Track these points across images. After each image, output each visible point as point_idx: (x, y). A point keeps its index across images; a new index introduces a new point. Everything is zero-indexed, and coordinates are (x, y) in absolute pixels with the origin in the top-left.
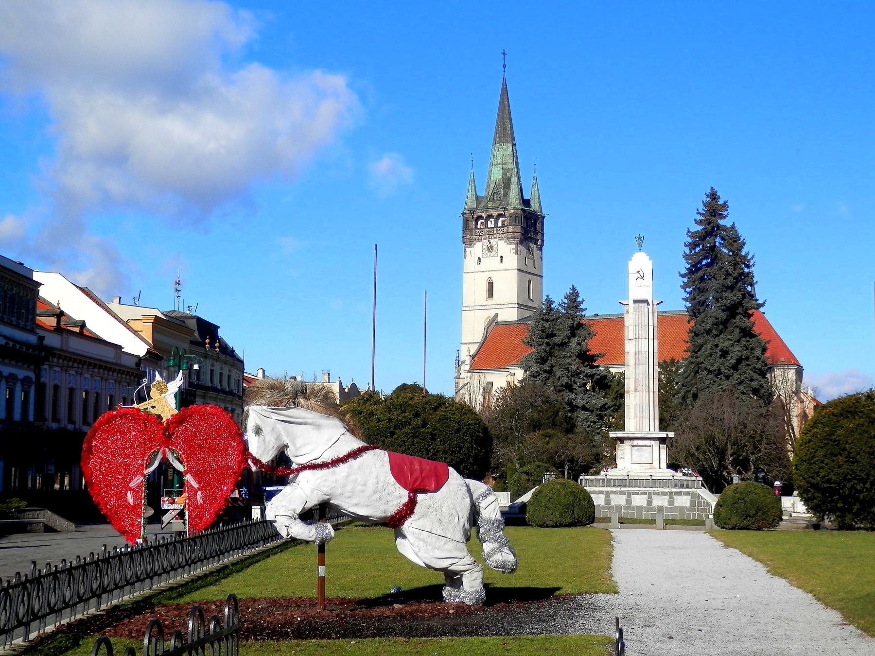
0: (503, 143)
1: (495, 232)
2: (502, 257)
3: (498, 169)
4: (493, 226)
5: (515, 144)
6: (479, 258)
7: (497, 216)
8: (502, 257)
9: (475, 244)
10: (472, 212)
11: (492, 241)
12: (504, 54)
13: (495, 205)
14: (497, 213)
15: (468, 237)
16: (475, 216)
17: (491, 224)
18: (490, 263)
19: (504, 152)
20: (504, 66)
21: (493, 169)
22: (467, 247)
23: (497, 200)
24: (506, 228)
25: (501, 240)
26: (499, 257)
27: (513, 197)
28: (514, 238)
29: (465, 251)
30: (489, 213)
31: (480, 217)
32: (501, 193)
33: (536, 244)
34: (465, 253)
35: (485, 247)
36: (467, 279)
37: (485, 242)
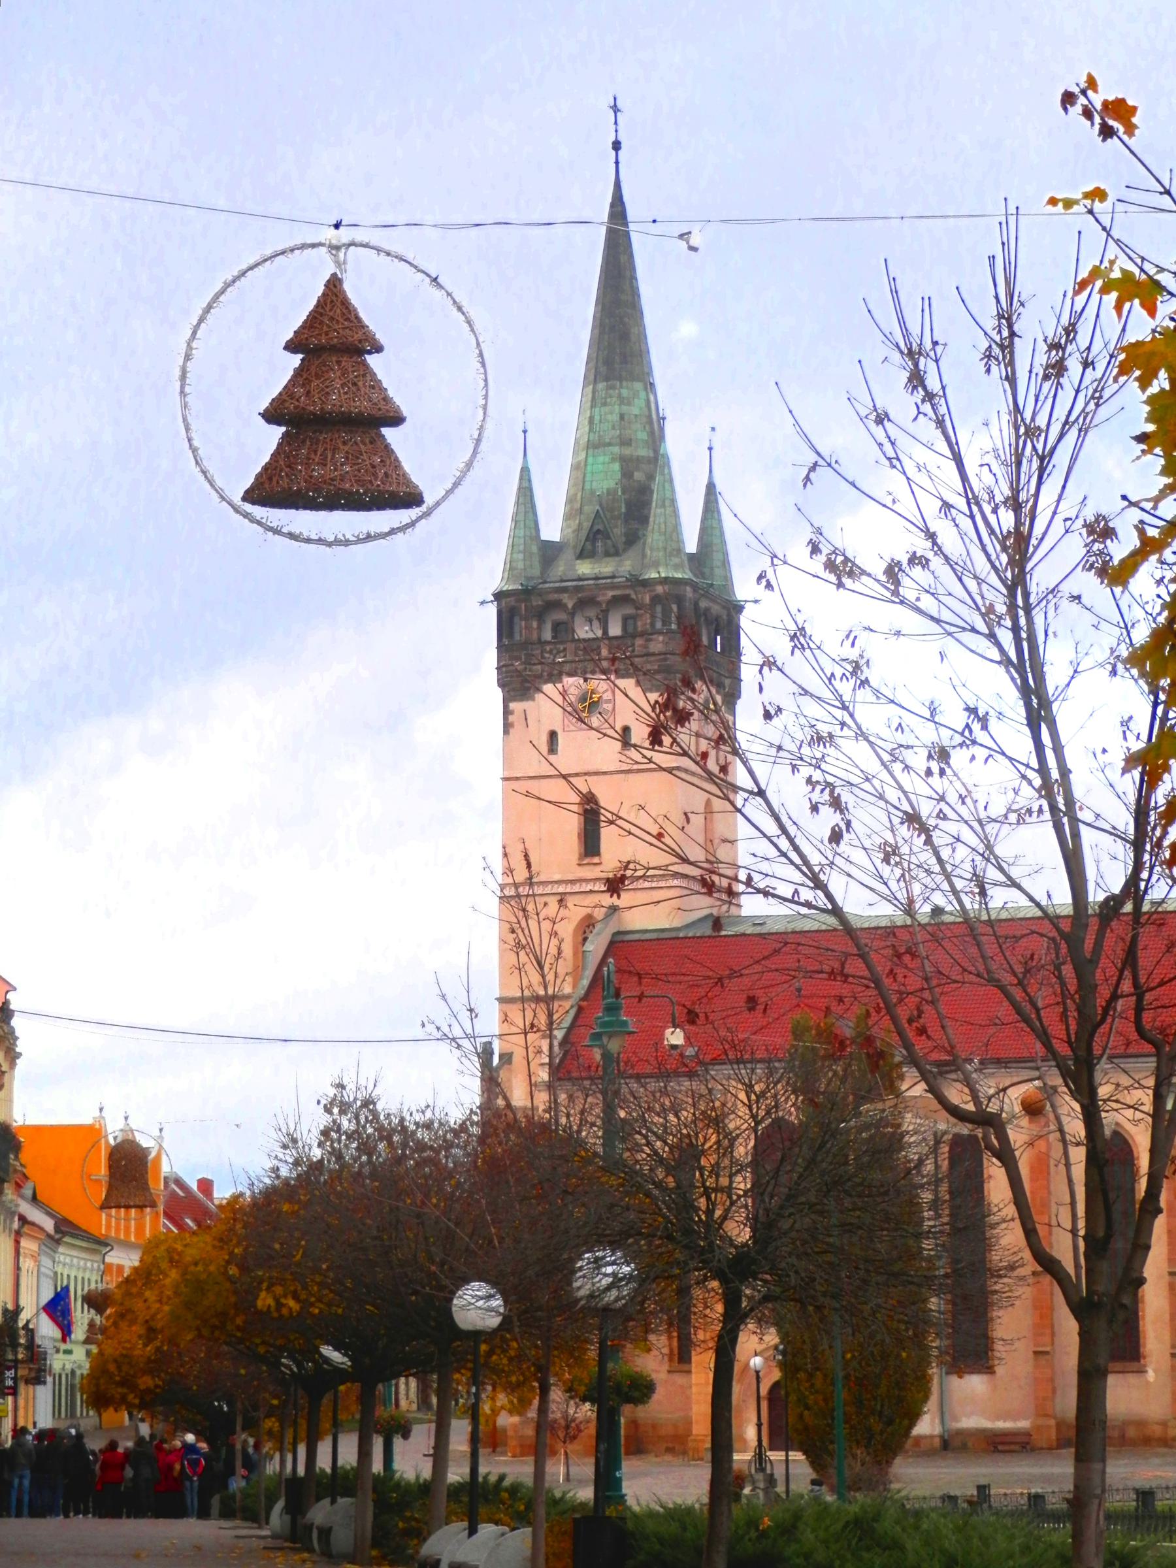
0: (620, 379)
3: (607, 459)
4: (599, 633)
6: (553, 735)
12: (615, 109)
13: (606, 567)
14: (610, 593)
16: (537, 602)
19: (625, 408)
20: (617, 146)
21: (590, 460)
22: (514, 699)
24: (639, 642)
27: (661, 545)
31: (558, 605)
32: (618, 532)
37: (572, 683)
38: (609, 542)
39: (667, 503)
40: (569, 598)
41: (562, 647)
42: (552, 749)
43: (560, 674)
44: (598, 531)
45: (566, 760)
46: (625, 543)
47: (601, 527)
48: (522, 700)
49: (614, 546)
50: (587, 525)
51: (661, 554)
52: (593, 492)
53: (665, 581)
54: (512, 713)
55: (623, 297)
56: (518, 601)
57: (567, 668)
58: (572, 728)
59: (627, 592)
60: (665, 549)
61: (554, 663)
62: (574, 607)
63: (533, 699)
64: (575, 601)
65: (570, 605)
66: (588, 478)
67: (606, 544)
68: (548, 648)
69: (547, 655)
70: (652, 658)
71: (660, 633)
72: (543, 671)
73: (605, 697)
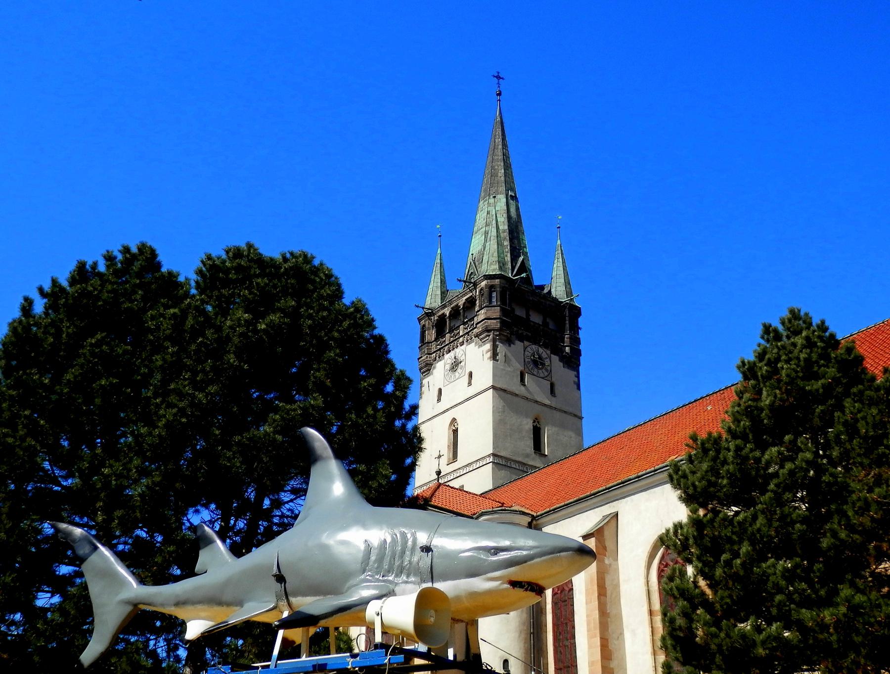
1: (461, 334)
3: (480, 236)
5: (514, 198)
6: (440, 390)
7: (464, 303)
8: (471, 375)
11: (459, 352)
12: (498, 77)
18: (457, 390)
20: (499, 94)
21: (473, 240)
26: (467, 376)
33: (557, 350)
34: (421, 390)
35: (448, 367)
37: (448, 358)
39: (492, 238)
42: (439, 400)
43: (443, 355)
45: (445, 403)
55: (496, 158)
57: (446, 348)
61: (440, 349)
64: (450, 309)
65: (448, 314)
66: (471, 250)
70: (478, 326)
72: (436, 356)
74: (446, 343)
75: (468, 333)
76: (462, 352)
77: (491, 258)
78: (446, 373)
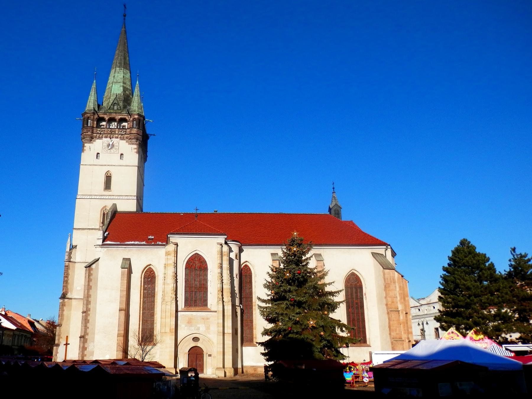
1: (117, 132)
2: (122, 154)
6: (98, 154)
8: (122, 154)
9: (94, 141)
10: (95, 112)
11: (114, 139)
14: (120, 117)
15: (89, 133)
16: (96, 116)
17: (114, 125)
22: (86, 143)
23: (118, 109)
24: (128, 130)
25: (122, 140)
28: (137, 139)
29: (84, 146)
30: (113, 115)
31: (103, 119)
32: (121, 104)
36: (83, 170)
37: (106, 141)
38: (119, 106)
40: (107, 117)
41: (103, 130)
44: (115, 103)
46: (123, 107)
47: (116, 102)
48: (89, 143)
49: (120, 107)
50: (111, 102)
51: (137, 108)
52: (114, 94)
53: (139, 114)
54: (86, 147)
56: (90, 115)
57: (104, 135)
58: (104, 152)
59: (125, 117)
60: (138, 107)
62: (108, 119)
63: (93, 144)
64: (109, 117)
65: (107, 119)
66: (113, 90)
67: (117, 107)
68: (99, 130)
69: (98, 132)
70: (132, 135)
71: (135, 128)
73: (116, 145)
74: (105, 133)
75: (122, 134)
76: (116, 142)
77: (139, 106)
78: (104, 147)
